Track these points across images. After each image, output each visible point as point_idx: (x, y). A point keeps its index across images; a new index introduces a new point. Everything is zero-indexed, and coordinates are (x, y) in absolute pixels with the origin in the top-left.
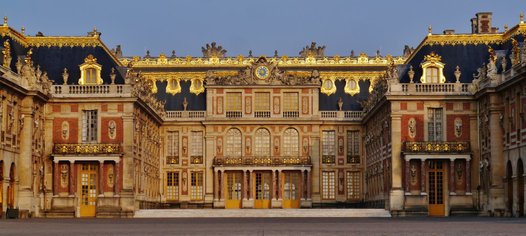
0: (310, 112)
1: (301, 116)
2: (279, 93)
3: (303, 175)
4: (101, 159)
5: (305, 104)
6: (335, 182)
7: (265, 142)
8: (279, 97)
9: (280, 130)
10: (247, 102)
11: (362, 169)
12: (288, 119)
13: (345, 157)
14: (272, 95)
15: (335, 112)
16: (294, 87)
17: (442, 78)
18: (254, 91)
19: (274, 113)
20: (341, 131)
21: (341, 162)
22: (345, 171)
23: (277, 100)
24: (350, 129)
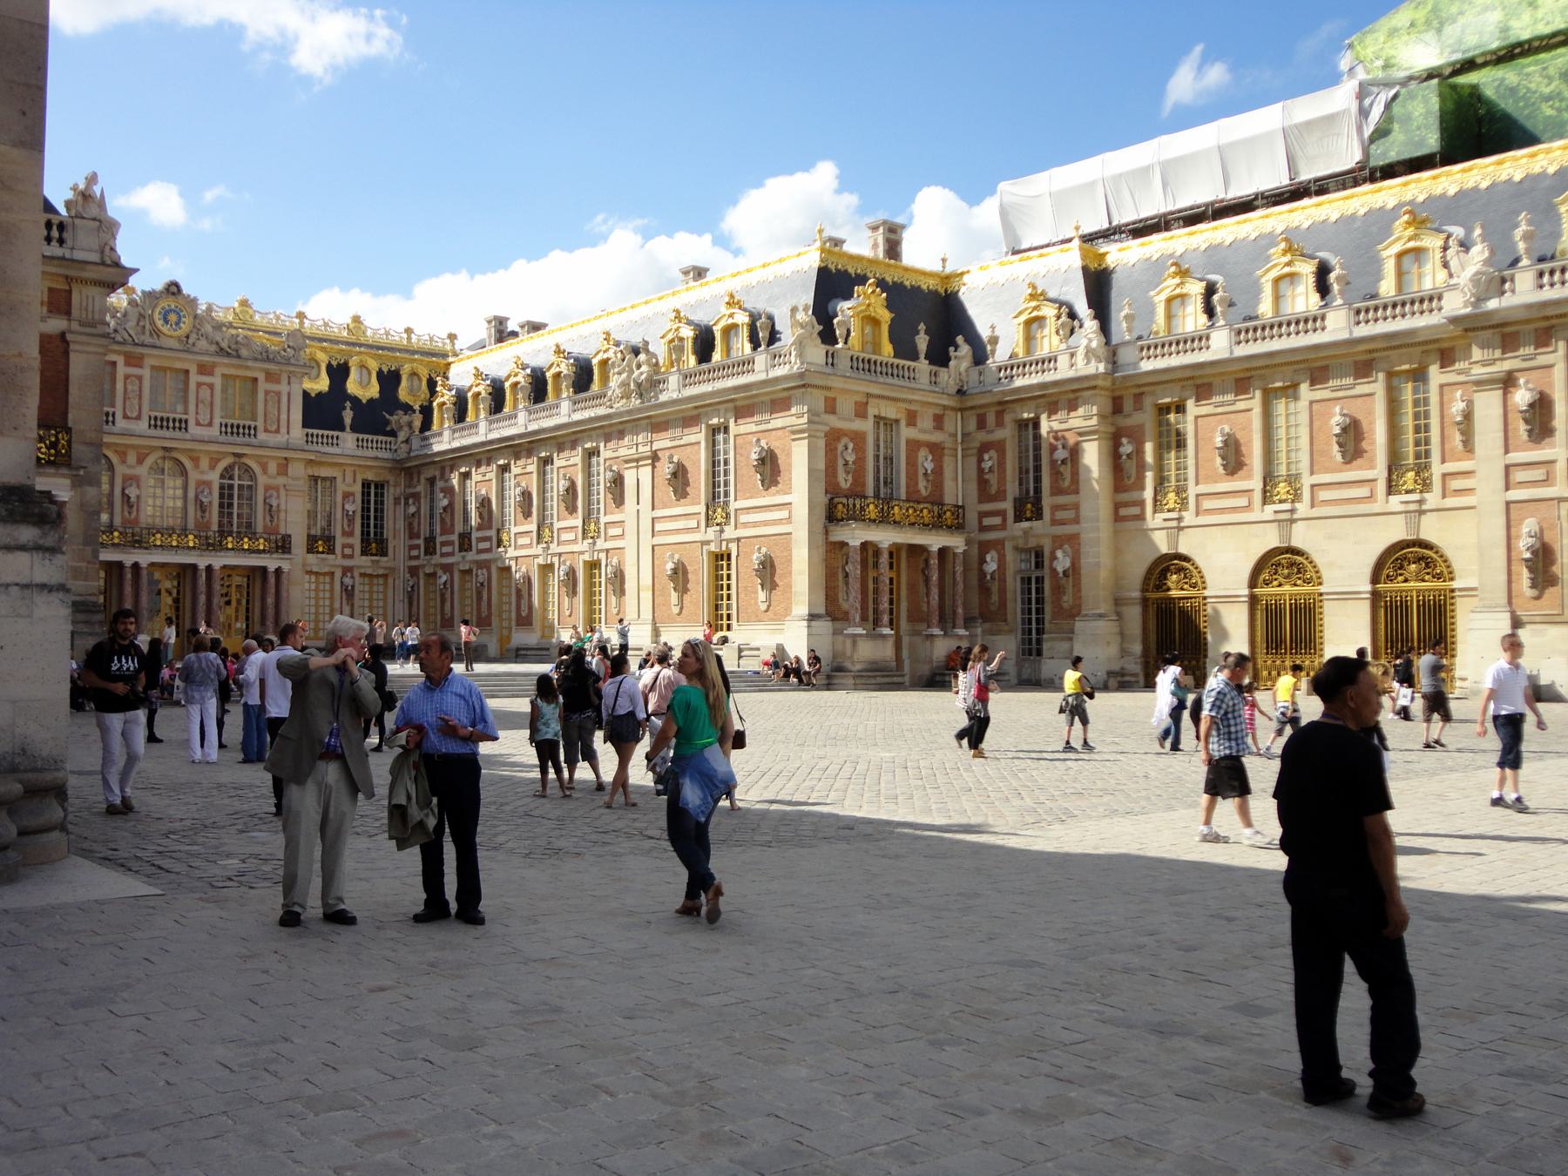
0: (283, 430)
1: (262, 436)
2: (211, 374)
3: (272, 580)
5: (273, 411)
6: (332, 599)
7: (171, 492)
8: (211, 386)
9: (212, 467)
10: (130, 387)
11: (393, 569)
12: (230, 438)
13: (356, 540)
14: (194, 378)
15: (335, 433)
16: (250, 363)
17: (888, 349)
18: (148, 362)
19: (198, 424)
20: (349, 479)
21: (348, 551)
22: (356, 574)
23: (205, 393)
24: (370, 476)
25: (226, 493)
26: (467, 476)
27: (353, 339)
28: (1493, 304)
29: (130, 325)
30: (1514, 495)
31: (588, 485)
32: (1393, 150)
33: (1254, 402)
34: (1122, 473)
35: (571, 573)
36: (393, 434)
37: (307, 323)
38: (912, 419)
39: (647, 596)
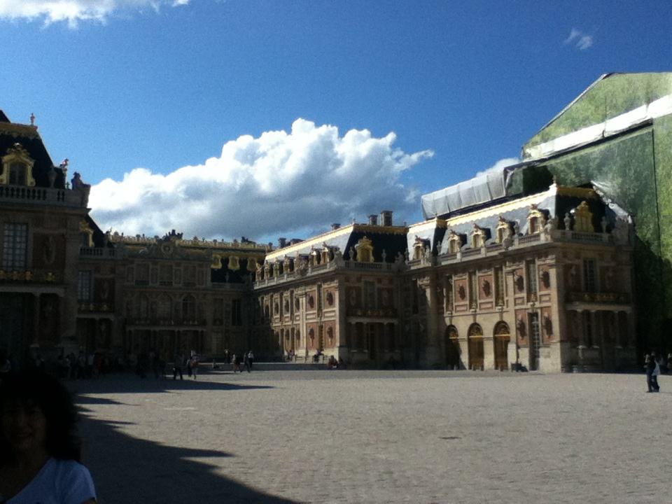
4: (97, 317)
17: (372, 258)
25: (185, 305)
26: (263, 298)
27: (234, 247)
28: (510, 248)
29: (154, 252)
30: (517, 307)
31: (292, 303)
32: (513, 191)
33: (466, 277)
34: (438, 298)
35: (288, 331)
36: (244, 282)
37: (217, 243)
38: (380, 281)
39: (305, 340)
